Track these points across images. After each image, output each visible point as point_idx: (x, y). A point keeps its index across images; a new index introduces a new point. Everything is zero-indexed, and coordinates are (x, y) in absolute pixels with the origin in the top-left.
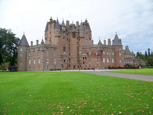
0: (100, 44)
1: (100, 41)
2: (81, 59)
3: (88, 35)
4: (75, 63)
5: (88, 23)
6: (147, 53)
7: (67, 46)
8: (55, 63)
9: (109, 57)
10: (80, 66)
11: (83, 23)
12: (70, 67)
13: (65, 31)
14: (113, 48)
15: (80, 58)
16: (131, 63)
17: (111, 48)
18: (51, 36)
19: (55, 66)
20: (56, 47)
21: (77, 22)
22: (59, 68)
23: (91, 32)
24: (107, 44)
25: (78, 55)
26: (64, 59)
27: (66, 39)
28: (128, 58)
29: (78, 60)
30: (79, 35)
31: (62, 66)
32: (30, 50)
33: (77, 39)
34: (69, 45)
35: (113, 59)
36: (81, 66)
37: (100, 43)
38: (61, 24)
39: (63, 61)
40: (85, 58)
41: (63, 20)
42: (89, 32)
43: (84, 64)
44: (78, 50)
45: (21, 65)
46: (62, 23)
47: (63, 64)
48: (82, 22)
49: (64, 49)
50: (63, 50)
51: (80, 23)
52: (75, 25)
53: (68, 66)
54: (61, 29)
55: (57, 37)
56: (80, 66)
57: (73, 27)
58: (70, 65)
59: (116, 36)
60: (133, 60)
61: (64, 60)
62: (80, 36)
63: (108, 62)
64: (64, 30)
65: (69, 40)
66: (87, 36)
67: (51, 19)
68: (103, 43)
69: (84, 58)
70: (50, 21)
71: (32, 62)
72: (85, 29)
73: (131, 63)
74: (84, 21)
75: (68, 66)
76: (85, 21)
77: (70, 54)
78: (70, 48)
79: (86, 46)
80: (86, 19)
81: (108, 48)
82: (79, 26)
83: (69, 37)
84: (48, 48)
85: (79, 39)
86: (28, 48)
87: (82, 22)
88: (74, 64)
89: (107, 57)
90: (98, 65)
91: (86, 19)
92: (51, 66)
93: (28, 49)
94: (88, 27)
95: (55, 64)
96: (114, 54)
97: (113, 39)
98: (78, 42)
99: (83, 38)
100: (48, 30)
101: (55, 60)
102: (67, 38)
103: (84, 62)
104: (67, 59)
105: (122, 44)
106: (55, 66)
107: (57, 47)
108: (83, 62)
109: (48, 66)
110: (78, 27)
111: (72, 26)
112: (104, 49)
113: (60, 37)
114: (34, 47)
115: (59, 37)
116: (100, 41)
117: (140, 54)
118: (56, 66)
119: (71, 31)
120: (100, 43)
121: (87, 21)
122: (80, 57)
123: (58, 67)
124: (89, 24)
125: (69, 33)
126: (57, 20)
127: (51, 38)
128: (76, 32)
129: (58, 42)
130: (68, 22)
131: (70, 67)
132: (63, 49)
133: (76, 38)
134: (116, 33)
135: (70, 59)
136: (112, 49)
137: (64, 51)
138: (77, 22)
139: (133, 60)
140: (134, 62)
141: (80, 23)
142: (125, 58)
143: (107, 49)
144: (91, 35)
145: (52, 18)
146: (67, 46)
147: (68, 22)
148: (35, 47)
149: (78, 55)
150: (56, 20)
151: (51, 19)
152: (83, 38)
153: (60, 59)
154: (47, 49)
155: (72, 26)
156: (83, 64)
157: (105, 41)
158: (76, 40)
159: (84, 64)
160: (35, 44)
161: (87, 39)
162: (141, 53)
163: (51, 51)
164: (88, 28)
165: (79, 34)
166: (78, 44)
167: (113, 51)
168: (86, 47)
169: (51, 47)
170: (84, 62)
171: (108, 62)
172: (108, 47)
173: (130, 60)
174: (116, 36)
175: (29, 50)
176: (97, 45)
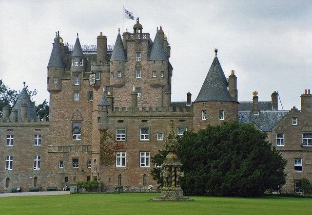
17: (169, 114)
19: (36, 178)
22: (51, 185)
26: (73, 156)
39: (71, 162)
41: (78, 39)
59: (216, 62)
76: (135, 29)
81: (146, 119)
89: (137, 150)
92: (20, 179)
99: (122, 86)
106: (36, 178)
107: (48, 123)
109: (8, 179)
112: (120, 121)
118: (39, 178)
121: (141, 28)
134: (216, 51)
153: (56, 158)
154: (8, 130)
167: (180, 124)
174: (216, 62)
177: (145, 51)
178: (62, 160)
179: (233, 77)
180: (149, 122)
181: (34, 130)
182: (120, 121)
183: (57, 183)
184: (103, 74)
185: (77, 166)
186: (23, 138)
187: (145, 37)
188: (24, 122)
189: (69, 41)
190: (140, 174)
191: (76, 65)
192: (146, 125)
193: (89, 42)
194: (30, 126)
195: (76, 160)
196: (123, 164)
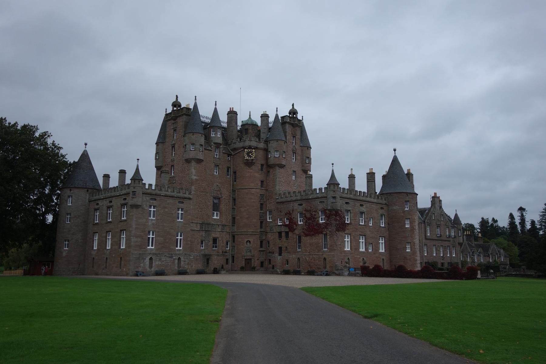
0: (332, 186)
1: (333, 176)
2: (272, 237)
3: (299, 158)
4: (250, 251)
5: (299, 117)
6: (517, 221)
8: (178, 248)
10: (266, 263)
11: (283, 118)
12: (233, 262)
13: (221, 144)
14: (380, 201)
15: (269, 235)
16: (451, 254)
17: (375, 201)
18: (173, 161)
20: (187, 195)
21: (265, 117)
23: (309, 148)
24: (361, 186)
25: (261, 223)
26: (214, 235)
27: (226, 170)
28: (439, 239)
29: (261, 242)
30: (267, 159)
31: (207, 259)
32: (100, 202)
33: (262, 170)
34: (234, 191)
35: (382, 241)
36: (270, 260)
37: (333, 183)
38: (208, 121)
39: (211, 242)
40: (283, 234)
41: (216, 109)
42: (304, 146)
43: (280, 254)
44: (264, 205)
45: (64, 254)
46: (210, 116)
47: (207, 252)
48: (277, 116)
49: (216, 201)
50: (211, 207)
51: (271, 119)
52: (256, 125)
53: (227, 260)
54: (207, 138)
55: (193, 163)
56: (266, 263)
57: (250, 131)
58: (233, 257)
60: (459, 244)
61: (215, 240)
62: (272, 161)
63: (362, 249)
64: (216, 141)
65: (235, 173)
66: (293, 162)
67: (176, 104)
68: (344, 184)
69: (280, 233)
70: (173, 110)
71: (102, 243)
72: (289, 137)
73: (451, 254)
74: (284, 112)
75: (227, 260)
76: (290, 113)
77: (234, 218)
78: (235, 199)
79: (289, 193)
80: (293, 105)
82: (270, 128)
83: (237, 163)
84: (158, 198)
85: (269, 172)
86: (95, 198)
87: (280, 116)
88: (249, 254)
90: (325, 259)
91: (293, 105)
93: (95, 200)
94: (298, 133)
95: (178, 252)
96: (388, 224)
97: (385, 173)
98: (262, 182)
100: (167, 140)
101: (179, 237)
102: (228, 168)
103: (280, 248)
104: (223, 237)
105: (416, 191)
106: (179, 259)
107: (191, 196)
108: (278, 248)
110: (266, 131)
111: (247, 130)
112: (347, 203)
113: (203, 163)
114: (108, 195)
115: (199, 161)
116: (333, 176)
117: (492, 224)
118: (182, 259)
119: (241, 145)
120: (333, 183)
122: (268, 230)
123: (188, 264)
124: (304, 121)
125: (234, 149)
126: (195, 106)
127: (173, 166)
128: (256, 148)
129: (194, 178)
130: (232, 114)
131: (233, 262)
132: (210, 204)
135: (234, 237)
136: (379, 206)
137: (216, 207)
138: (265, 117)
139: (459, 244)
140: (462, 252)
141: (271, 119)
142: (426, 239)
143: (361, 205)
144: (309, 158)
145: (179, 100)
146: (225, 194)
147: (232, 114)
148: (113, 194)
149: (264, 225)
150: (191, 107)
151: (176, 104)
152: (282, 166)
154: (152, 199)
155: (247, 127)
156: (277, 255)
157: (352, 177)
158: (257, 175)
159: (280, 254)
160: (114, 182)
161: (294, 171)
162: (495, 221)
163: (166, 208)
164: (298, 136)
165: (267, 155)
166: (262, 186)
168: (289, 199)
169: (166, 196)
170: (280, 248)
171: (362, 249)
172: (364, 199)
173: (447, 244)
175: (97, 202)
176: (323, 191)
177: (298, 136)
178: (204, 239)
179: (409, 175)
180: (364, 206)
181: (177, 202)
182: (347, 203)
183: (200, 265)
184: (260, 151)
185: (216, 247)
186: (166, 210)
188: (168, 191)
190: (360, 258)
191: (216, 136)
192: (363, 209)
194: (160, 195)
196: (152, 246)
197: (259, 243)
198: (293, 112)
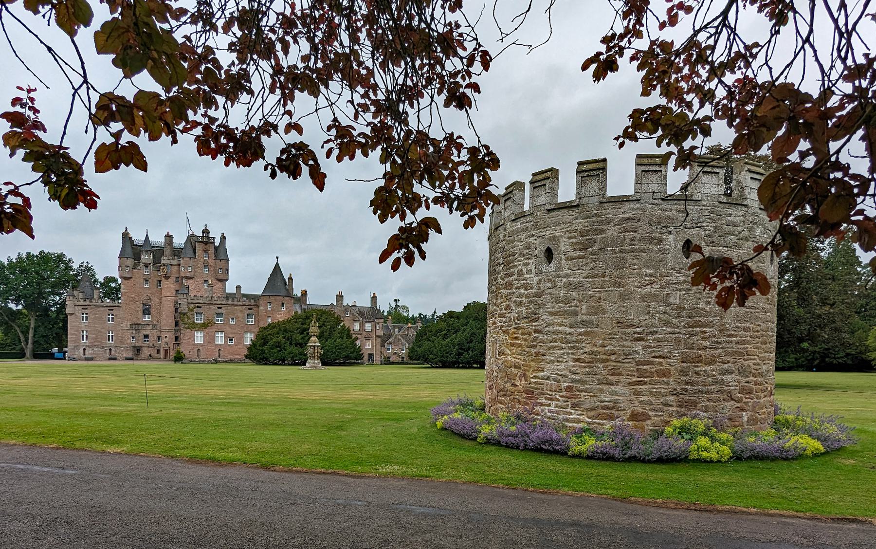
7: (155, 301)
9: (228, 329)
27: (156, 283)
31: (138, 350)
39: (142, 337)
47: (137, 345)
62: (182, 274)
76: (203, 232)
106: (110, 350)
109: (85, 349)
118: (113, 349)
121: (208, 233)
132: (140, 309)
133: (173, 279)
174: (277, 267)
179: (290, 279)
187: (211, 240)
189: (138, 237)
191: (146, 258)
192: (220, 311)
193: (157, 239)
195: (146, 336)
197: (174, 337)
198: (206, 231)
